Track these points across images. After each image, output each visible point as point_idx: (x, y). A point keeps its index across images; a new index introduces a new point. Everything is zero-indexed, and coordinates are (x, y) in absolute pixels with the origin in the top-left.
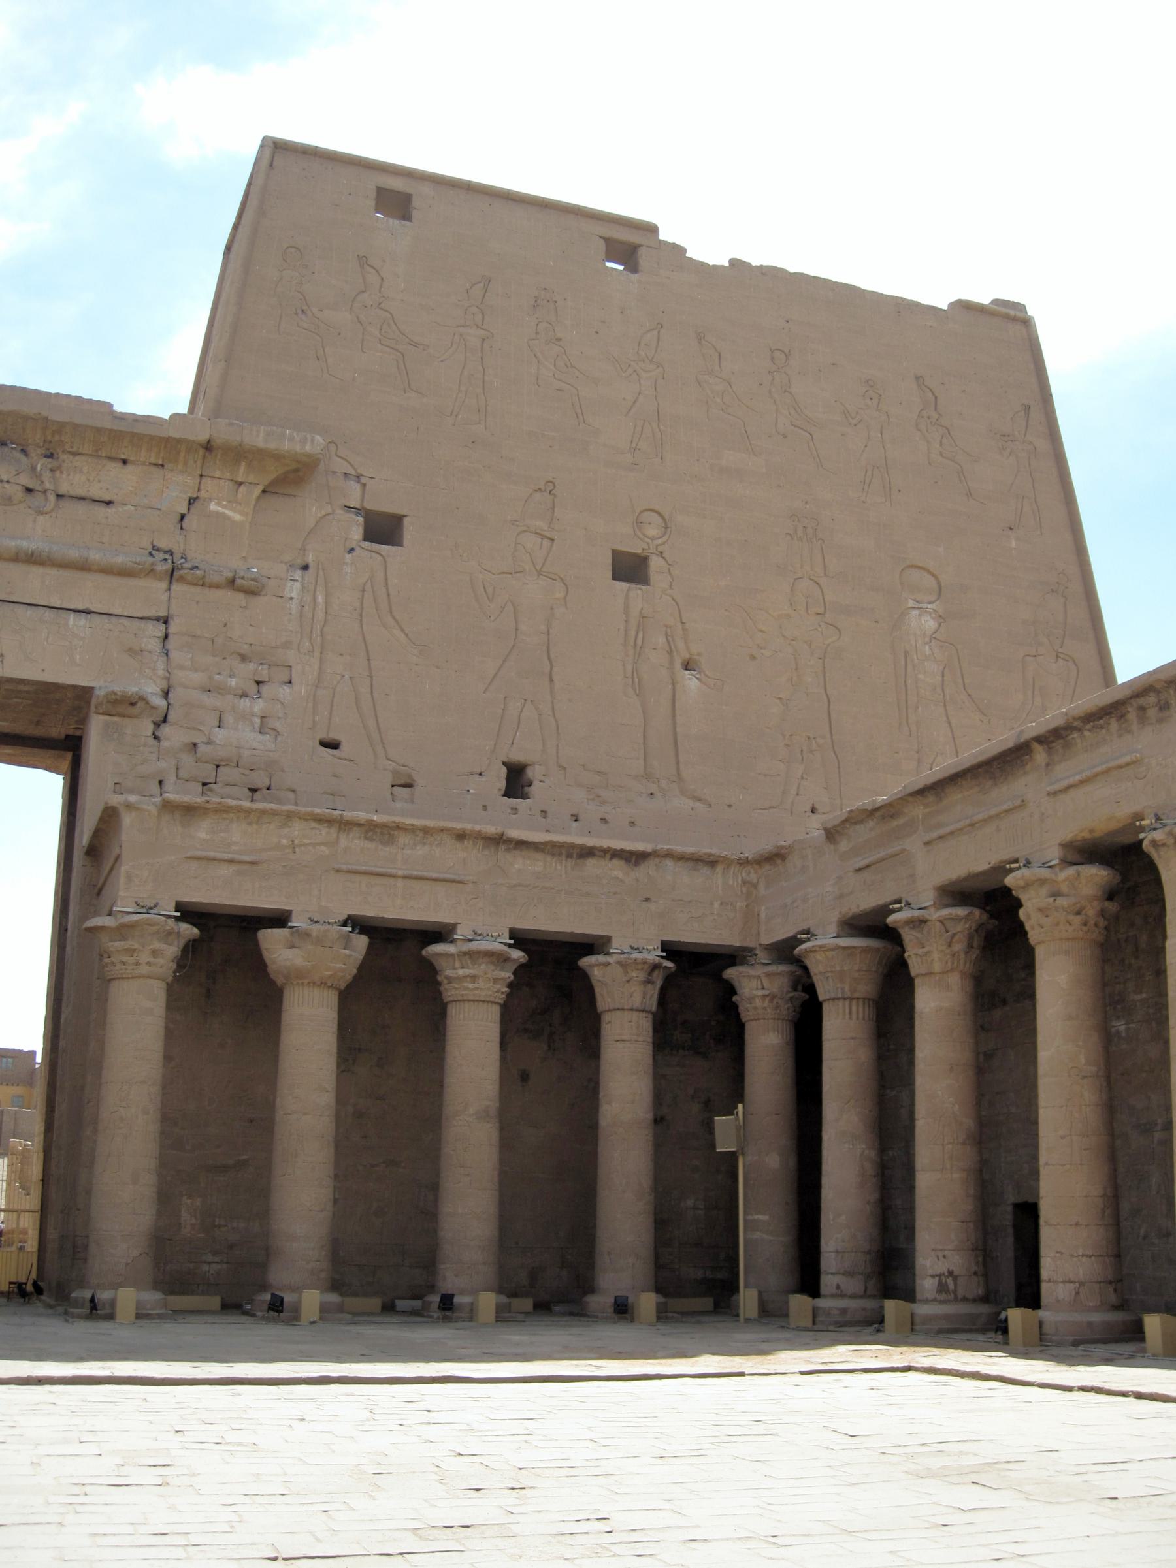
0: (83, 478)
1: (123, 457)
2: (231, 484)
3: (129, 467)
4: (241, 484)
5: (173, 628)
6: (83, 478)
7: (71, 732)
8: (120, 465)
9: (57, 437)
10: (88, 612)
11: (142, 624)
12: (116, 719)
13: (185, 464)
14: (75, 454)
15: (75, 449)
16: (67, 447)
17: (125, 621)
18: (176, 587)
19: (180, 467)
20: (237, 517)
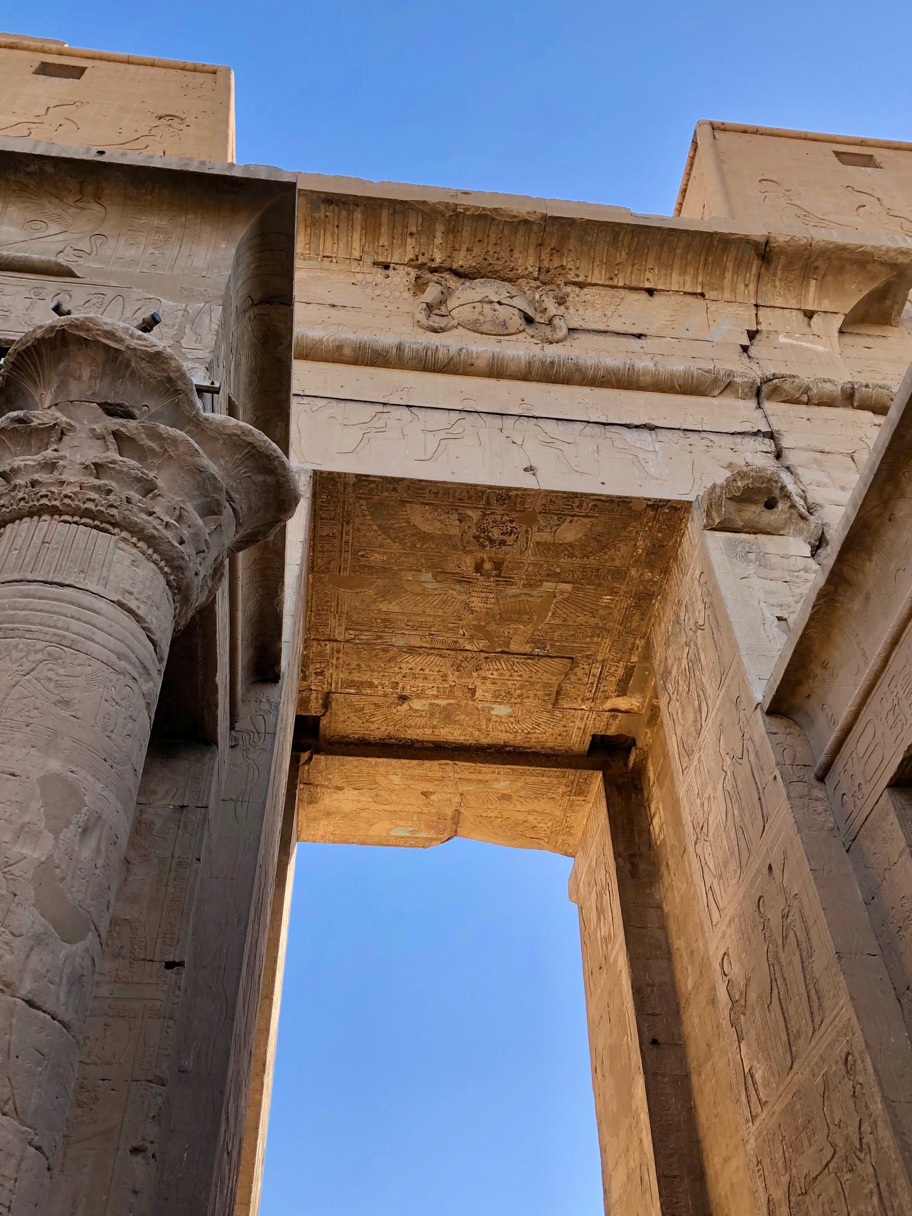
0: (598, 313)
1: (647, 285)
2: (800, 315)
3: (657, 299)
4: (809, 315)
5: (785, 443)
6: (598, 313)
7: (600, 729)
8: (644, 296)
9: (556, 263)
10: (651, 428)
11: (738, 439)
12: (743, 536)
13: (734, 290)
14: (581, 285)
15: (581, 279)
16: (571, 277)
17: (712, 437)
18: (767, 405)
19: (727, 295)
20: (820, 349)
